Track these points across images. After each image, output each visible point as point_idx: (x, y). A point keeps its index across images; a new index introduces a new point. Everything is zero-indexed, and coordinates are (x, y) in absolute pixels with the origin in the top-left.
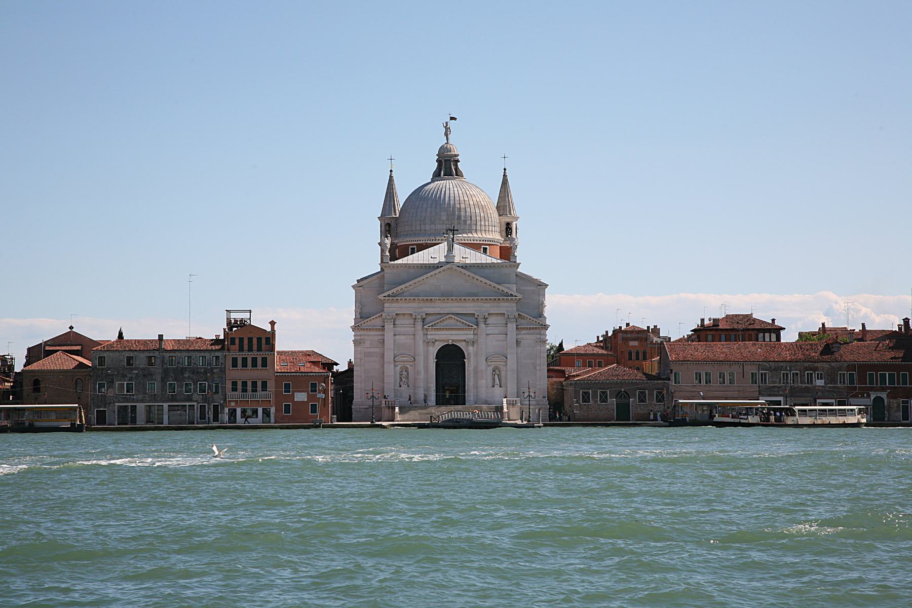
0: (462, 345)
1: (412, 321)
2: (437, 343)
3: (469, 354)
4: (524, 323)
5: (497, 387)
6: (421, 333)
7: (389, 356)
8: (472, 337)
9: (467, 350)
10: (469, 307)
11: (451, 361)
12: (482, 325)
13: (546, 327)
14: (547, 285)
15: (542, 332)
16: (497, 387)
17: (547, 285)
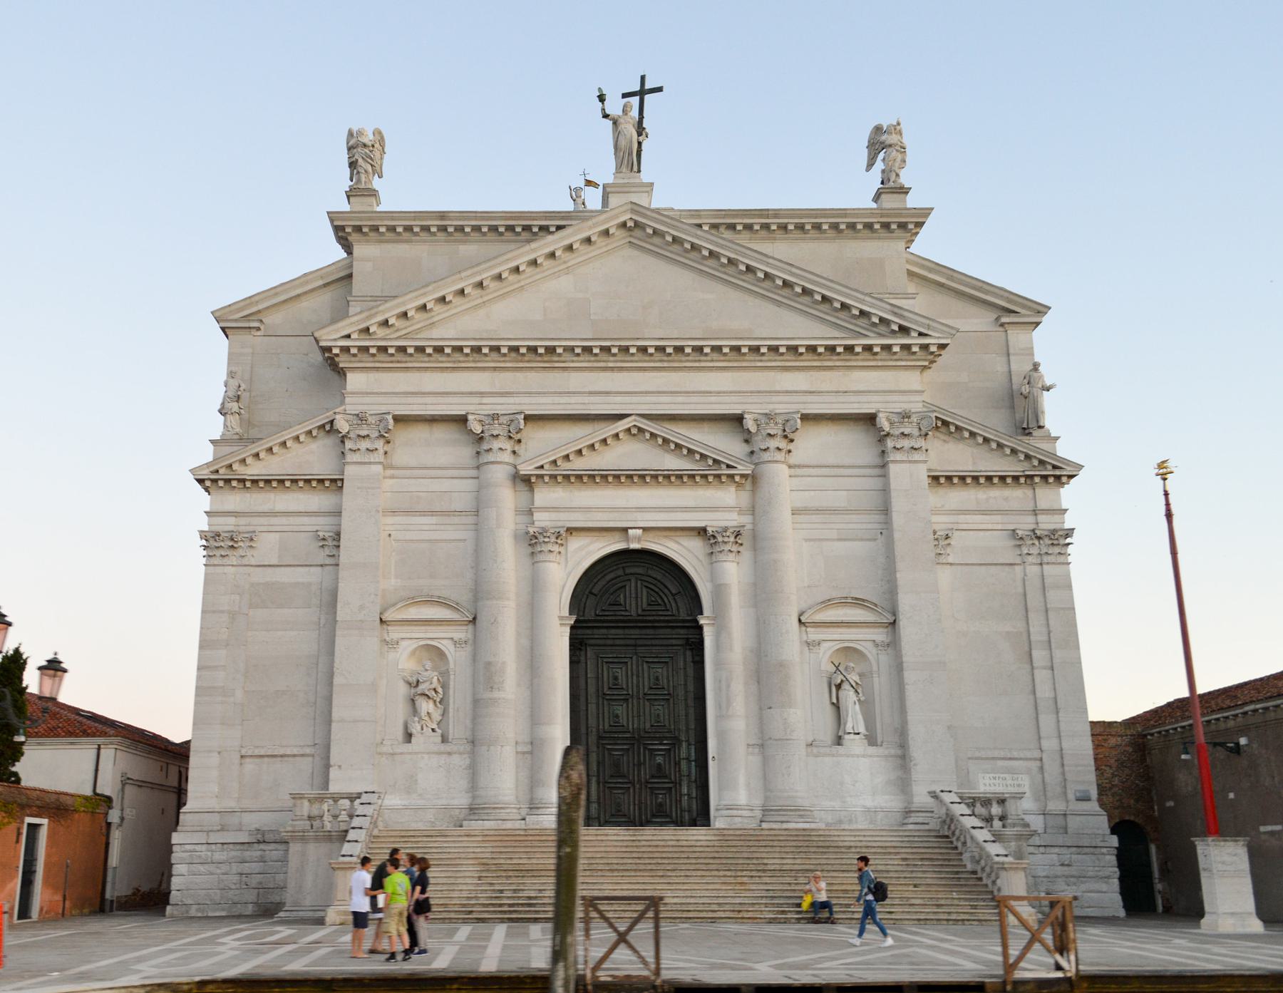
0: (685, 553)
1: (464, 453)
2: (575, 543)
3: (719, 591)
4: (959, 457)
5: (855, 745)
6: (507, 499)
7: (355, 599)
8: (732, 520)
9: (713, 576)
10: (717, 388)
11: (638, 625)
12: (779, 474)
13: (1057, 473)
14: (1041, 310)
15: (1044, 495)
16: (855, 745)
17: (1041, 310)
